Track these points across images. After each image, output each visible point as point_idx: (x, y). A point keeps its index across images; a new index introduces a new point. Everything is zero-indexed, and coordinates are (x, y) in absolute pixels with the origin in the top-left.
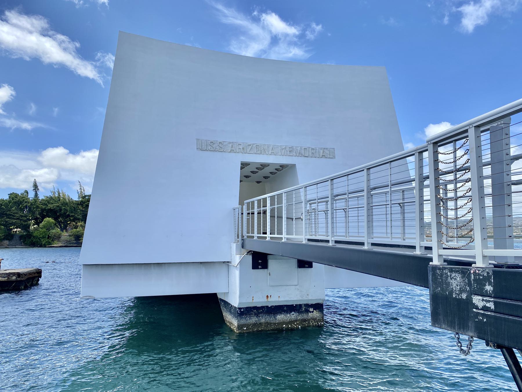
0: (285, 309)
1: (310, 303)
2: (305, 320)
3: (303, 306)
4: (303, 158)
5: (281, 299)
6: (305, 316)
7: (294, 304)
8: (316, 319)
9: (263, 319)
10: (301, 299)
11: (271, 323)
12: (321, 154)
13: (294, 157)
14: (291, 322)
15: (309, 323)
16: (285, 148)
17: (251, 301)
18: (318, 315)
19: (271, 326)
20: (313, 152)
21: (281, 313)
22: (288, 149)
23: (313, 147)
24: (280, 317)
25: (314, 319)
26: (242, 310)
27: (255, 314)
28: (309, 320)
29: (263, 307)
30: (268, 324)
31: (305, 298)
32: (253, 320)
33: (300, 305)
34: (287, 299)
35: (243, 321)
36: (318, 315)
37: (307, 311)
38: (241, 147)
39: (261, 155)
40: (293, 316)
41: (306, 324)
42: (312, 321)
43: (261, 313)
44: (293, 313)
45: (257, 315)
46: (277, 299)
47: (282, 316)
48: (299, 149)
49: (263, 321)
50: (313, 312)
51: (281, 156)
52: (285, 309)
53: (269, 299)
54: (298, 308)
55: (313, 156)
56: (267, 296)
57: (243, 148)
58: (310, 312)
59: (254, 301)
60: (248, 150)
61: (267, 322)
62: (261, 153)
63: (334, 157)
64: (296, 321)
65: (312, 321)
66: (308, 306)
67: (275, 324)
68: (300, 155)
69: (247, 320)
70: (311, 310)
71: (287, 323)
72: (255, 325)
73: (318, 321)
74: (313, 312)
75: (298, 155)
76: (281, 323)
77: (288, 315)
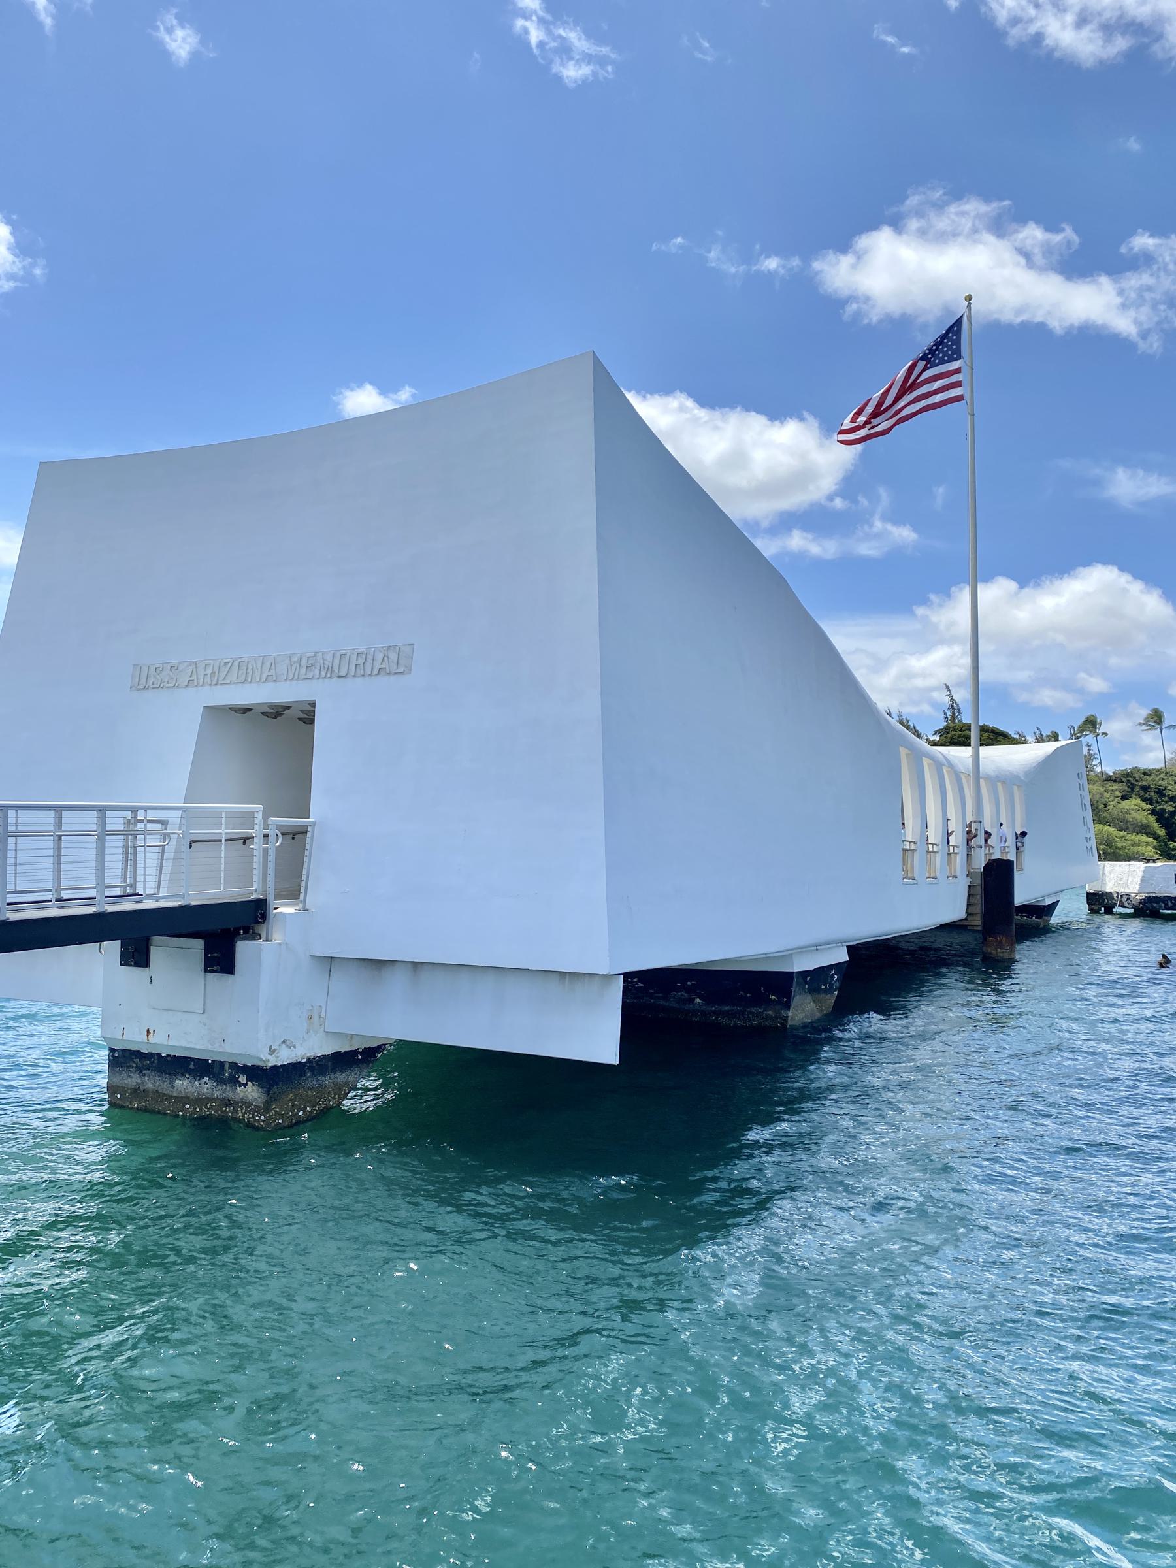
1: (242, 1061)
2: (228, 1103)
3: (227, 1066)
6: (227, 1092)
7: (211, 1058)
9: (152, 1082)
10: (210, 1047)
12: (377, 666)
13: (315, 681)
14: (201, 1101)
22: (304, 663)
24: (183, 1085)
27: (138, 1068)
29: (151, 1055)
33: (222, 1064)
35: (117, 1081)
37: (234, 1081)
40: (205, 1087)
44: (206, 1079)
45: (140, 1070)
48: (329, 657)
49: (150, 1086)
52: (192, 1066)
53: (152, 1039)
54: (216, 1070)
56: (148, 1031)
57: (213, 673)
58: (241, 1085)
63: (407, 671)
64: (210, 1099)
66: (237, 1068)
68: (330, 673)
73: (254, 1111)
74: (245, 1085)
75: (323, 674)
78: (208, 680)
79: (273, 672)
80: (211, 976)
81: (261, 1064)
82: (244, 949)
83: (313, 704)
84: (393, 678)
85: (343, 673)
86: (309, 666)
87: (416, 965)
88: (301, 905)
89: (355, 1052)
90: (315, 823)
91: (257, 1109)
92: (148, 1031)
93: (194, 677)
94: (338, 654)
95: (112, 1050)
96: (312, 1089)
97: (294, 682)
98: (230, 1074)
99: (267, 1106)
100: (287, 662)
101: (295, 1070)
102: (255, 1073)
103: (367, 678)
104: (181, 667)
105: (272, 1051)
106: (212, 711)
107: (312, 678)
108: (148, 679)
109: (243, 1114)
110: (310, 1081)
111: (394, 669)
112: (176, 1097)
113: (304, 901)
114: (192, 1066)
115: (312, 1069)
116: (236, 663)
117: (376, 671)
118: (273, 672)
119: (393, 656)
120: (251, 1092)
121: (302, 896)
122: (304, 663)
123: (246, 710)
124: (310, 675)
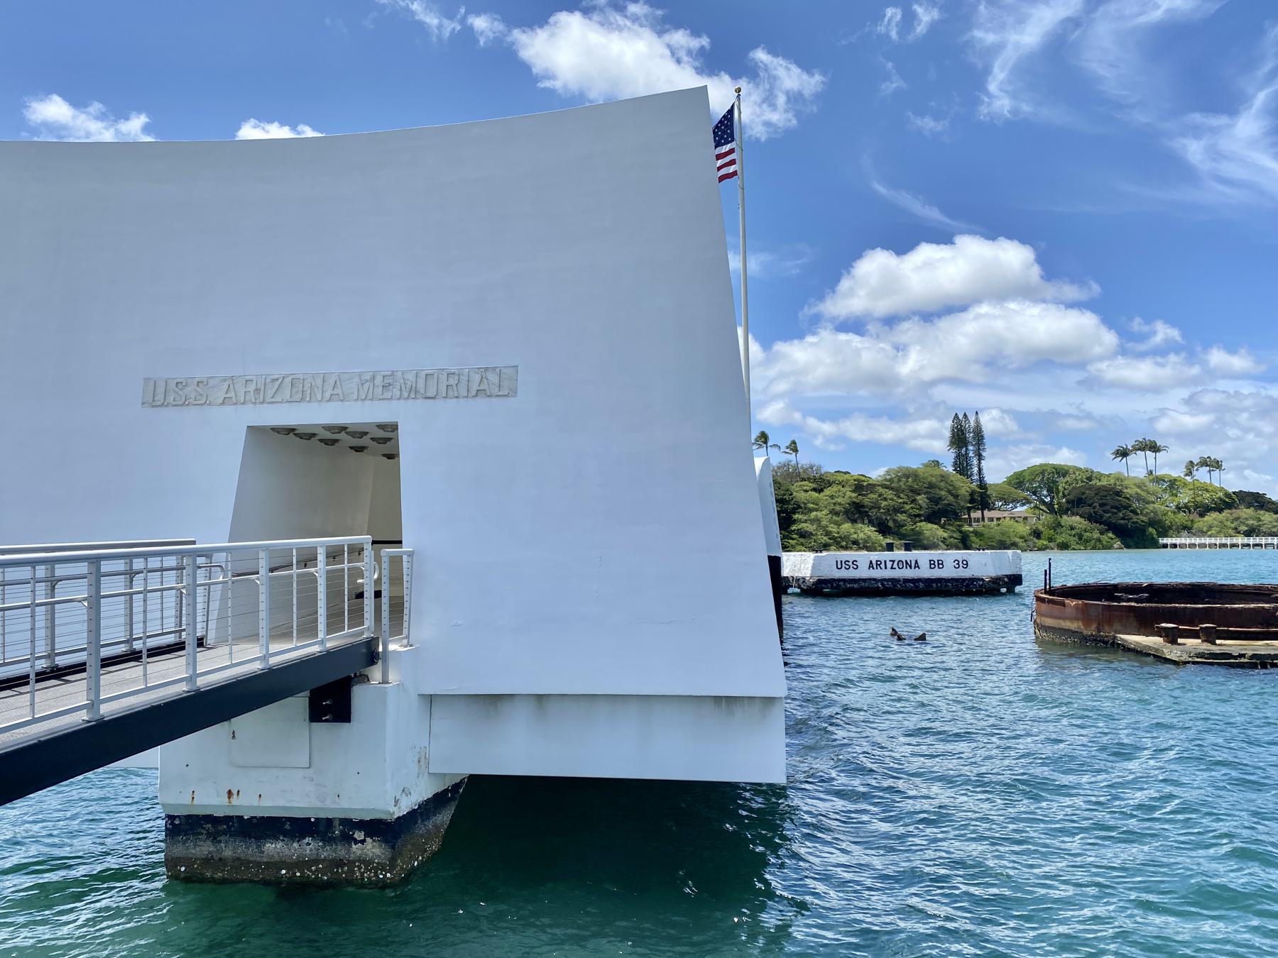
0: (287, 827)
1: (356, 817)
2: (339, 863)
3: (336, 823)
4: (420, 401)
5: (266, 802)
6: (341, 852)
8: (371, 862)
9: (230, 849)
10: (319, 804)
11: (250, 862)
12: (474, 388)
13: (394, 402)
14: (302, 864)
15: (351, 871)
16: (374, 378)
17: (188, 801)
18: (377, 851)
19: (248, 868)
20: (453, 381)
21: (277, 839)
22: (379, 380)
23: (453, 369)
24: (274, 848)
25: (367, 863)
26: (177, 822)
27: (209, 834)
28: (351, 863)
29: (227, 819)
30: (239, 862)
31: (329, 804)
32: (204, 848)
34: (281, 803)
35: (179, 850)
36: (377, 851)
37: (348, 839)
38: (252, 387)
39: (303, 405)
40: (309, 847)
41: (343, 872)
42: (360, 868)
43: (225, 833)
44: (306, 840)
45: (214, 838)
46: (255, 802)
47: (279, 845)
48: (411, 377)
49: (228, 853)
50: (363, 842)
51: (359, 403)
53: (235, 801)
54: (322, 828)
55: (450, 393)
56: (230, 793)
57: (257, 390)
58: (356, 842)
59: (196, 802)
60: (270, 393)
61: (238, 859)
62: (302, 400)
63: (513, 393)
64: (316, 861)
65: (360, 868)
66: (350, 824)
67: (258, 864)
68: (413, 393)
69: (188, 848)
70: (359, 835)
71: (291, 866)
72: (207, 861)
73: (376, 869)
74: (363, 842)
75: (406, 395)
76: (275, 864)
77: (295, 845)
78: (251, 396)
79: (338, 391)
80: (315, 724)
81: (384, 817)
82: (359, 694)
83: (394, 427)
84: (494, 400)
85: (431, 393)
86: (387, 385)
87: (540, 698)
88: (405, 641)
89: (446, 791)
90: (410, 554)
91: (382, 867)
92: (230, 793)
93: (232, 394)
94: (423, 374)
95: (170, 818)
96: (422, 836)
97: (368, 403)
98: (341, 832)
99: (393, 861)
100: (356, 380)
101: (412, 816)
102: (376, 828)
103: (461, 400)
104: (212, 383)
105: (396, 802)
106: (255, 432)
107: (391, 398)
108: (163, 395)
109: (362, 874)
110: (421, 829)
111: (496, 391)
112: (267, 863)
113: (408, 637)
114: (287, 827)
115: (422, 814)
116: (288, 380)
117: (474, 393)
118: (338, 391)
119: (493, 378)
120: (372, 849)
121: (405, 631)
122: (379, 380)
123: (290, 431)
124: (388, 395)
